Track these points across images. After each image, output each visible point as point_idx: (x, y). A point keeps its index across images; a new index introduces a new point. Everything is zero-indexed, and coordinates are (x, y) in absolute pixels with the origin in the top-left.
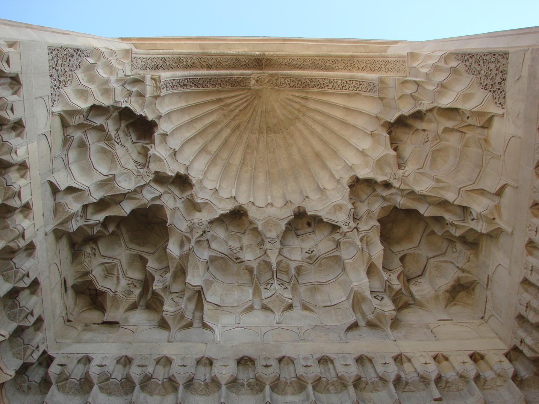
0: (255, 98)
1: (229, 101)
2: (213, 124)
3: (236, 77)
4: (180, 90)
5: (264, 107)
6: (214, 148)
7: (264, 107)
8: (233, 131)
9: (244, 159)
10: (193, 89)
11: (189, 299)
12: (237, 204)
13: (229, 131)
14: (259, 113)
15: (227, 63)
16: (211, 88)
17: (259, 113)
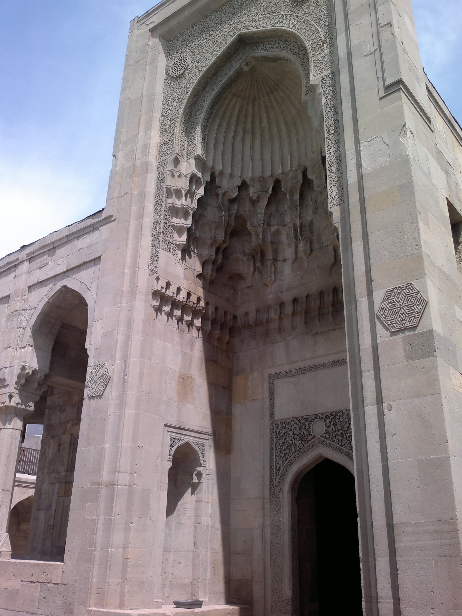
0: (253, 74)
1: (240, 89)
2: (240, 111)
3: (233, 76)
4: (210, 120)
5: (261, 76)
6: (249, 126)
7: (261, 76)
8: (253, 104)
9: (269, 119)
10: (216, 108)
11: (271, 267)
12: (274, 179)
13: (251, 106)
14: (261, 83)
15: (223, 62)
16: (225, 95)
17: (261, 83)
